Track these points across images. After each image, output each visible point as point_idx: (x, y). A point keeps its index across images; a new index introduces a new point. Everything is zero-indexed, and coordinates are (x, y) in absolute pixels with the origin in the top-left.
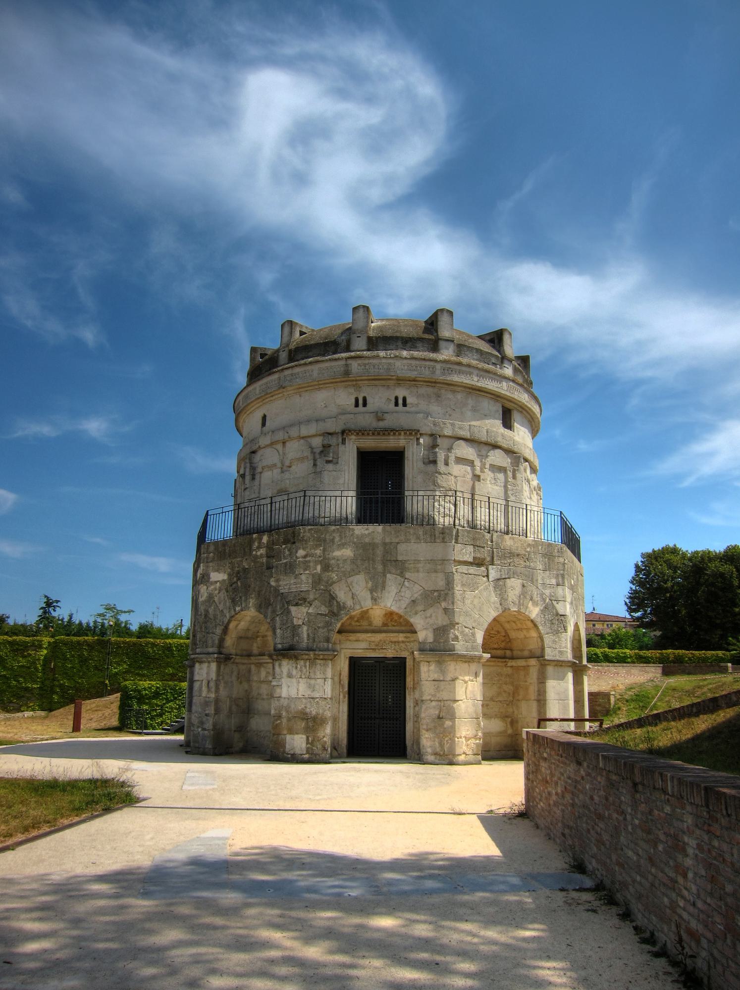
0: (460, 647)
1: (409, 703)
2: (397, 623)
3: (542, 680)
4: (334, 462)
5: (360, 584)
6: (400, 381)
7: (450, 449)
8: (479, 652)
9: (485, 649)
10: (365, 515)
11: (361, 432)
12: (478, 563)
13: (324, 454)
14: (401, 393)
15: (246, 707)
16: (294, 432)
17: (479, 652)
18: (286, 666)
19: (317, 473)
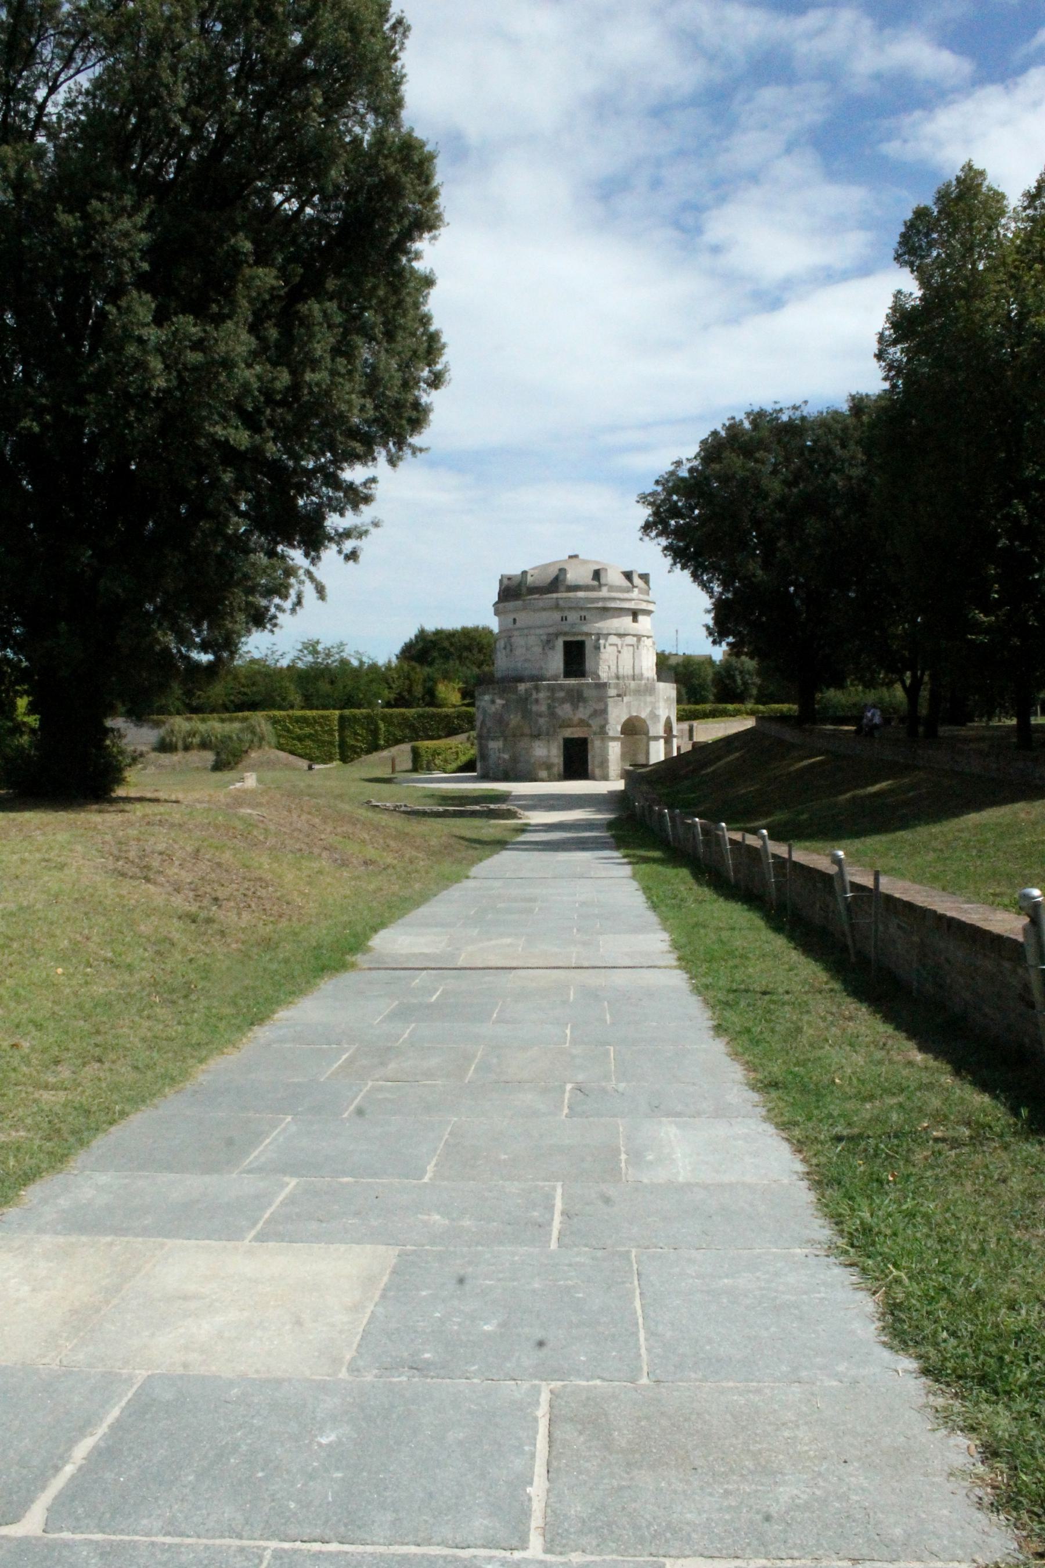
0: (611, 734)
1: (589, 757)
2: (582, 723)
3: (648, 745)
4: (553, 648)
5: (567, 707)
6: (582, 609)
7: (606, 640)
8: (619, 735)
9: (622, 733)
10: (568, 673)
11: (565, 634)
12: (619, 696)
13: (548, 643)
14: (583, 614)
15: (515, 759)
16: (532, 631)
17: (619, 735)
18: (537, 744)
19: (544, 654)
